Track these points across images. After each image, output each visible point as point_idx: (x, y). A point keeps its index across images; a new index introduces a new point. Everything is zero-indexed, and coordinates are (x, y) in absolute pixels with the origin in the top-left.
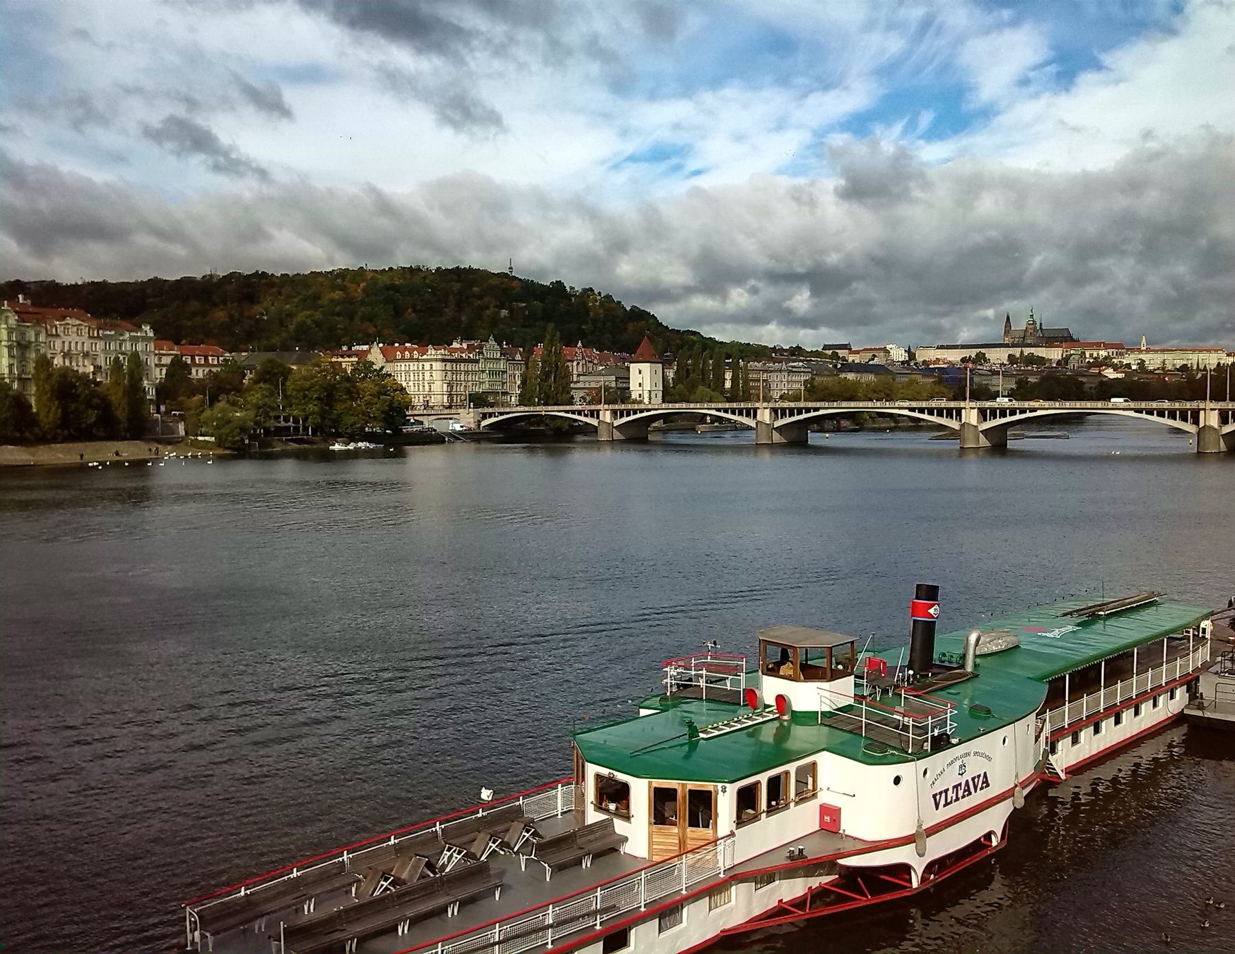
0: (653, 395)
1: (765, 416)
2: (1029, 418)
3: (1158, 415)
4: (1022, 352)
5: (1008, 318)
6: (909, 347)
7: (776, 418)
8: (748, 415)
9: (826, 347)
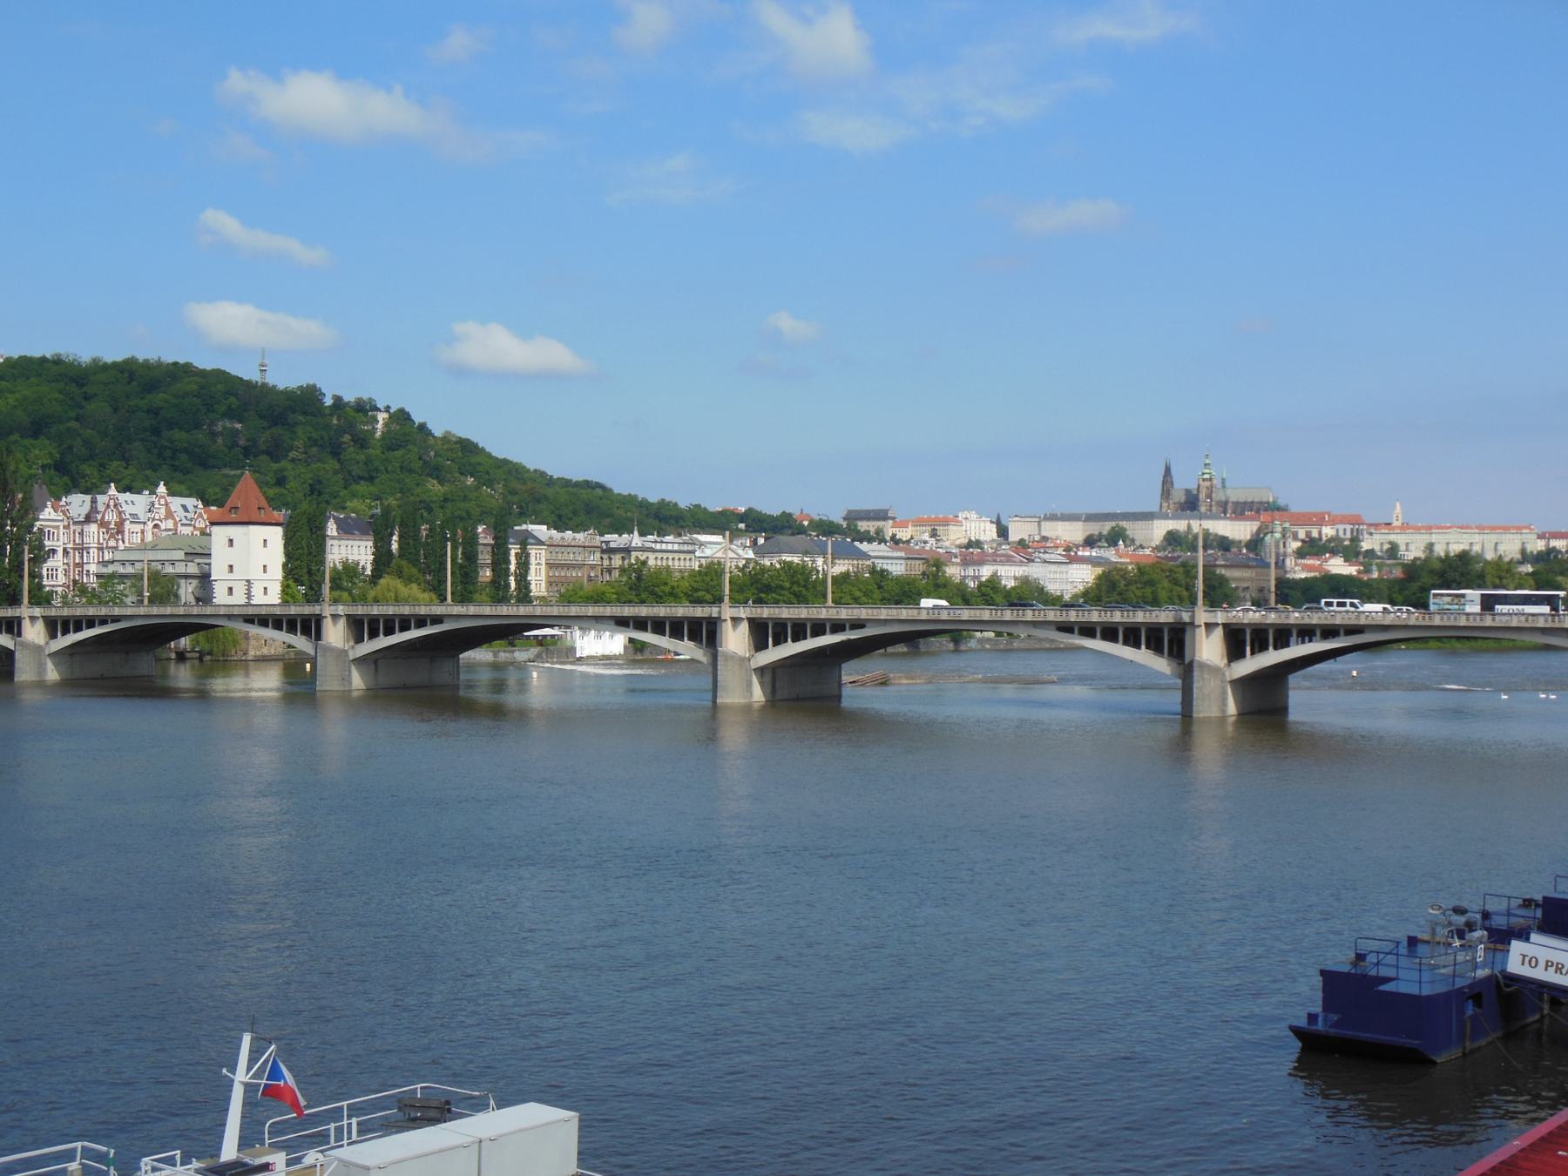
0: (257, 591)
1: (34, 633)
4: (1189, 527)
5: (1168, 470)
6: (998, 517)
9: (853, 517)
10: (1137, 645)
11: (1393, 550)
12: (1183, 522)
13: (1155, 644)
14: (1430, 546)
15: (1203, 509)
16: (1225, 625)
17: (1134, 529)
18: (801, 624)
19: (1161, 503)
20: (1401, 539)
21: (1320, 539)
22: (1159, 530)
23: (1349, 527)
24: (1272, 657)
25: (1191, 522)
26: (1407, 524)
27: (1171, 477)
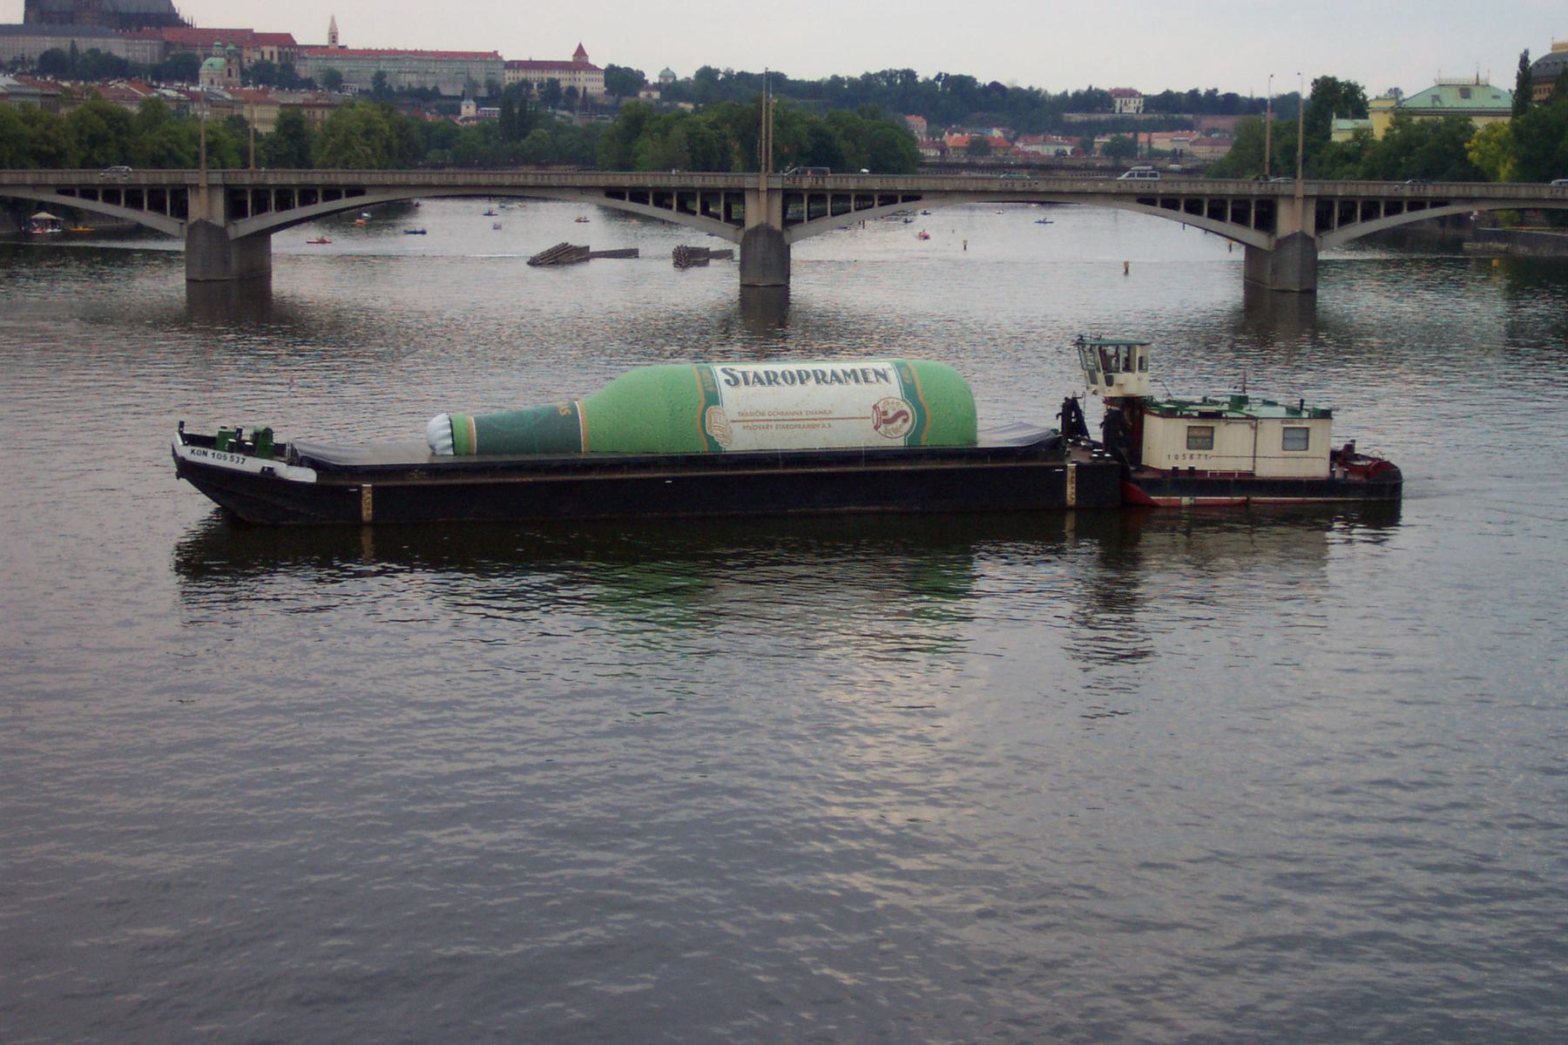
8: (157, 206)
12: (63, 39)
14: (380, 77)
18: (1173, 200)
23: (275, 49)
25: (76, 39)
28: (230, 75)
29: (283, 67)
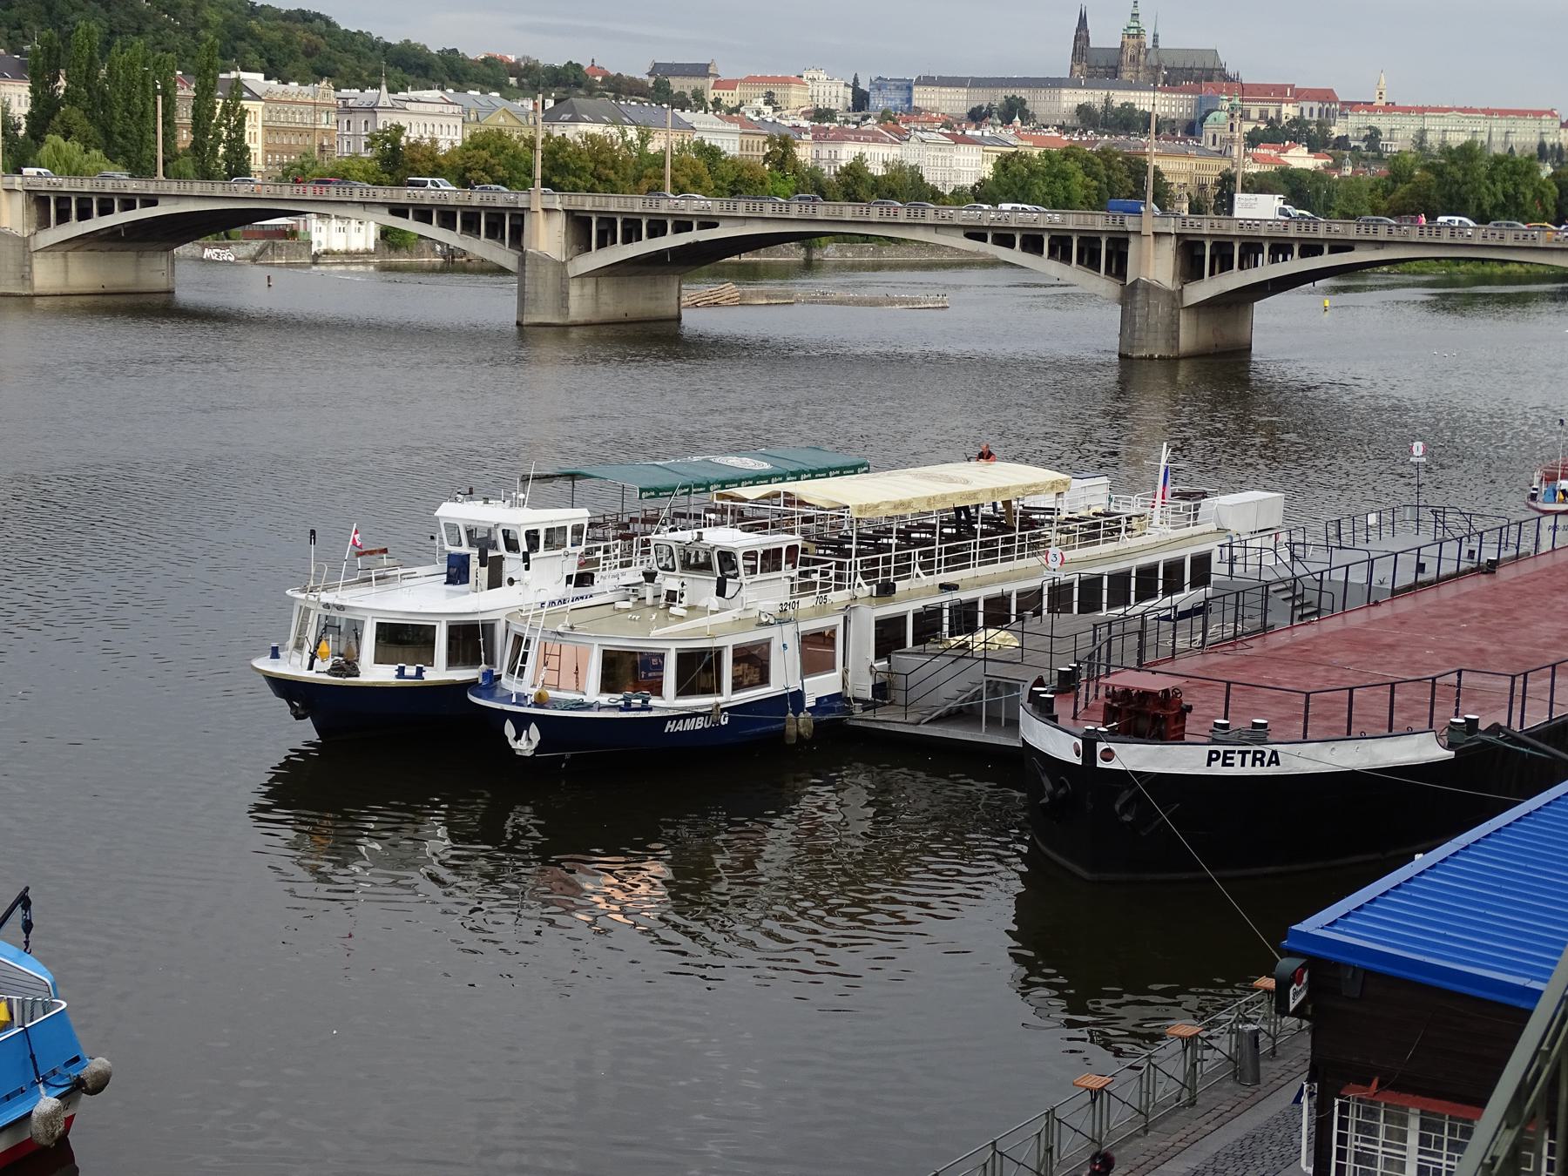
2: (697, 243)
3: (1024, 248)
4: (1108, 101)
5: (1083, 21)
6: (856, 80)
7: (44, 223)
10: (1066, 258)
11: (1373, 136)
12: (1097, 92)
13: (1089, 258)
14: (1422, 133)
15: (1126, 76)
16: (1179, 236)
17: (1038, 102)
19: (1072, 66)
20: (1382, 123)
21: (1279, 121)
22: (1071, 99)
23: (1316, 106)
24: (1235, 279)
26: (1393, 104)
27: (1087, 32)
28: (1232, 130)
29: (1319, 124)
